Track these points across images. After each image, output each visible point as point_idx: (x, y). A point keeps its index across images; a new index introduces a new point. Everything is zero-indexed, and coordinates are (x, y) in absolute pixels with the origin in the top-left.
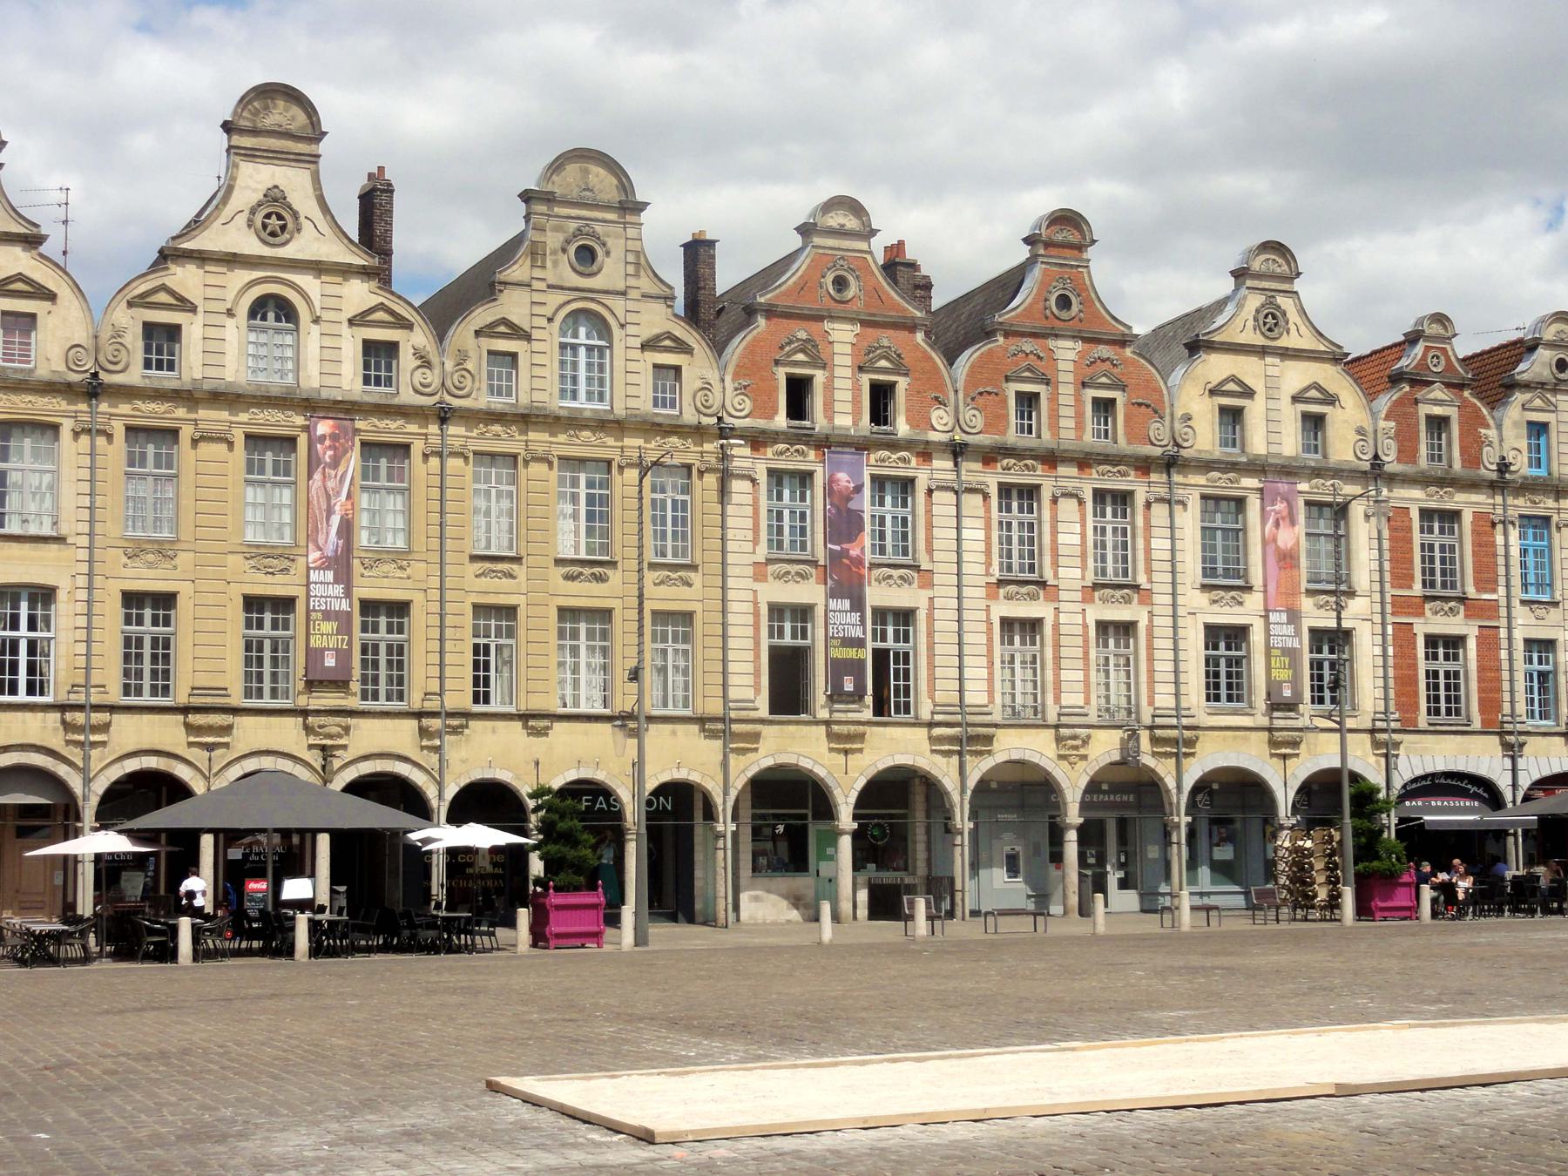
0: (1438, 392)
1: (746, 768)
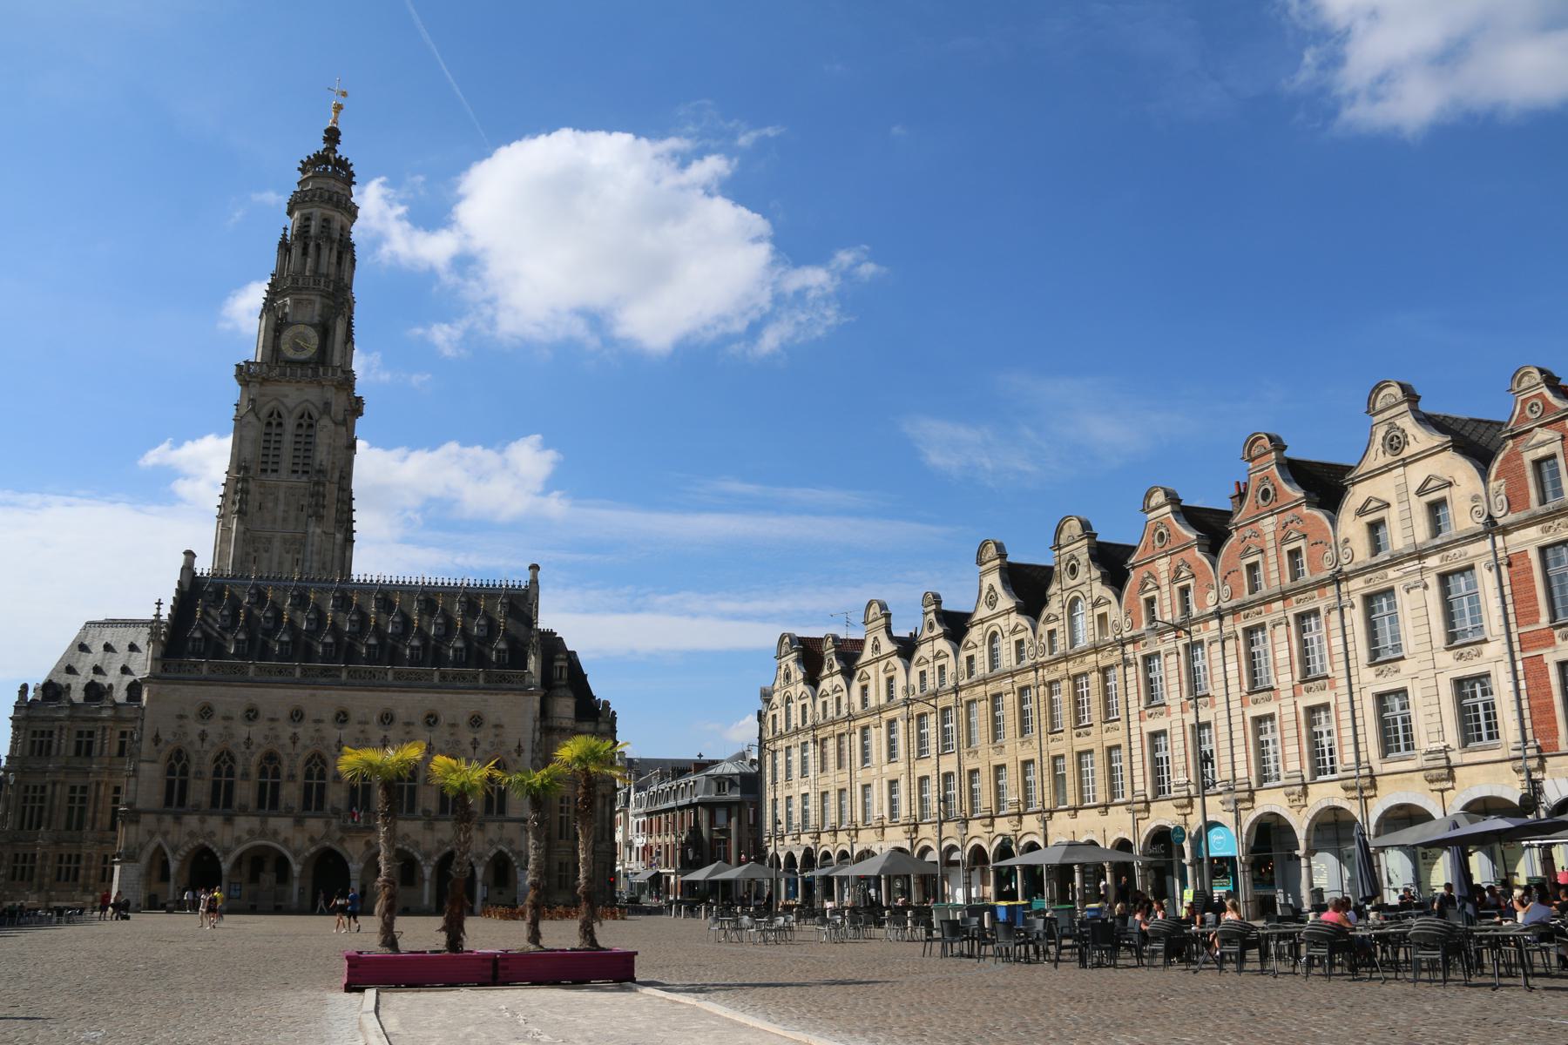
0: (1542, 435)
1: (1147, 826)
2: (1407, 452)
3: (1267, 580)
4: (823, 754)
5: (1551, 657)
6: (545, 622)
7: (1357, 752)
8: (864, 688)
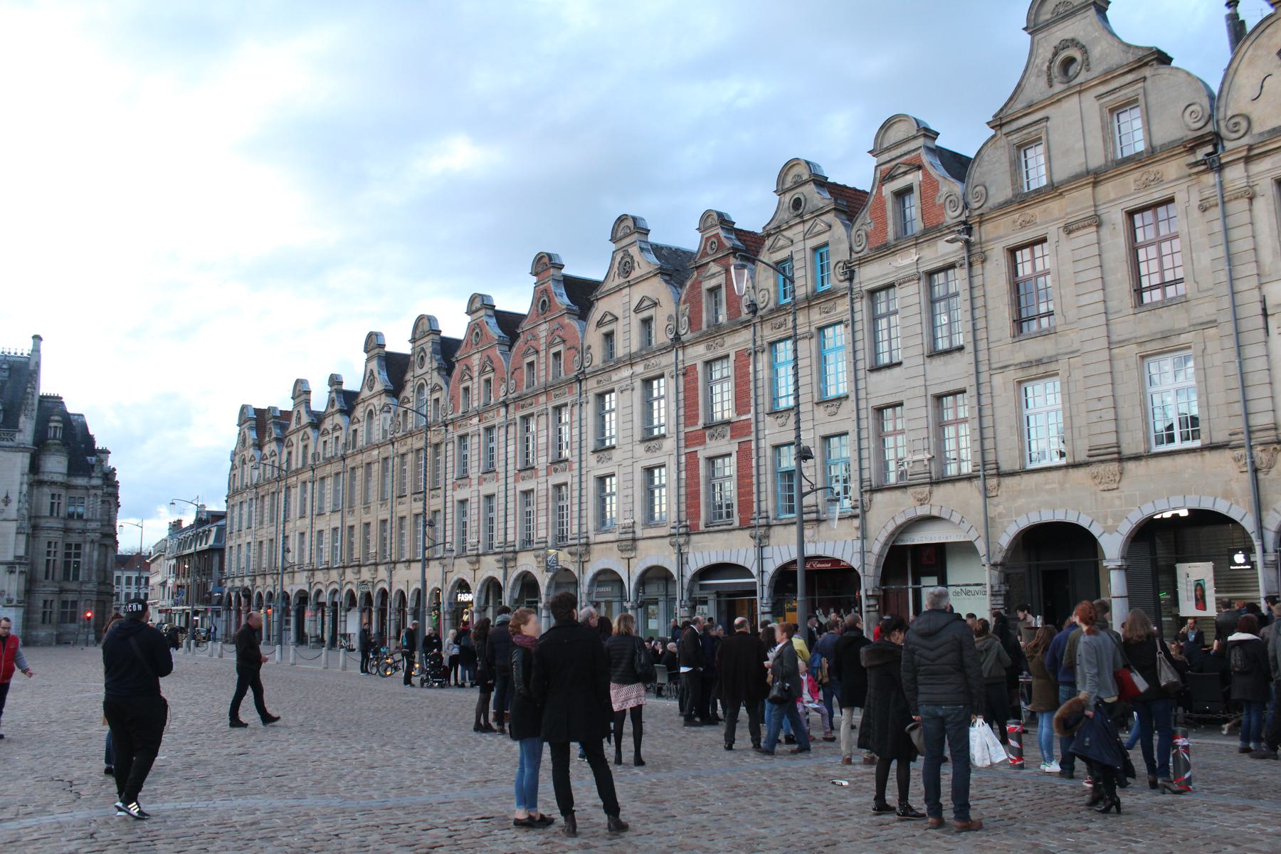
2: (634, 275)
3: (538, 377)
4: (262, 507)
5: (702, 453)
6: (47, 386)
7: (580, 525)
8: (290, 453)
